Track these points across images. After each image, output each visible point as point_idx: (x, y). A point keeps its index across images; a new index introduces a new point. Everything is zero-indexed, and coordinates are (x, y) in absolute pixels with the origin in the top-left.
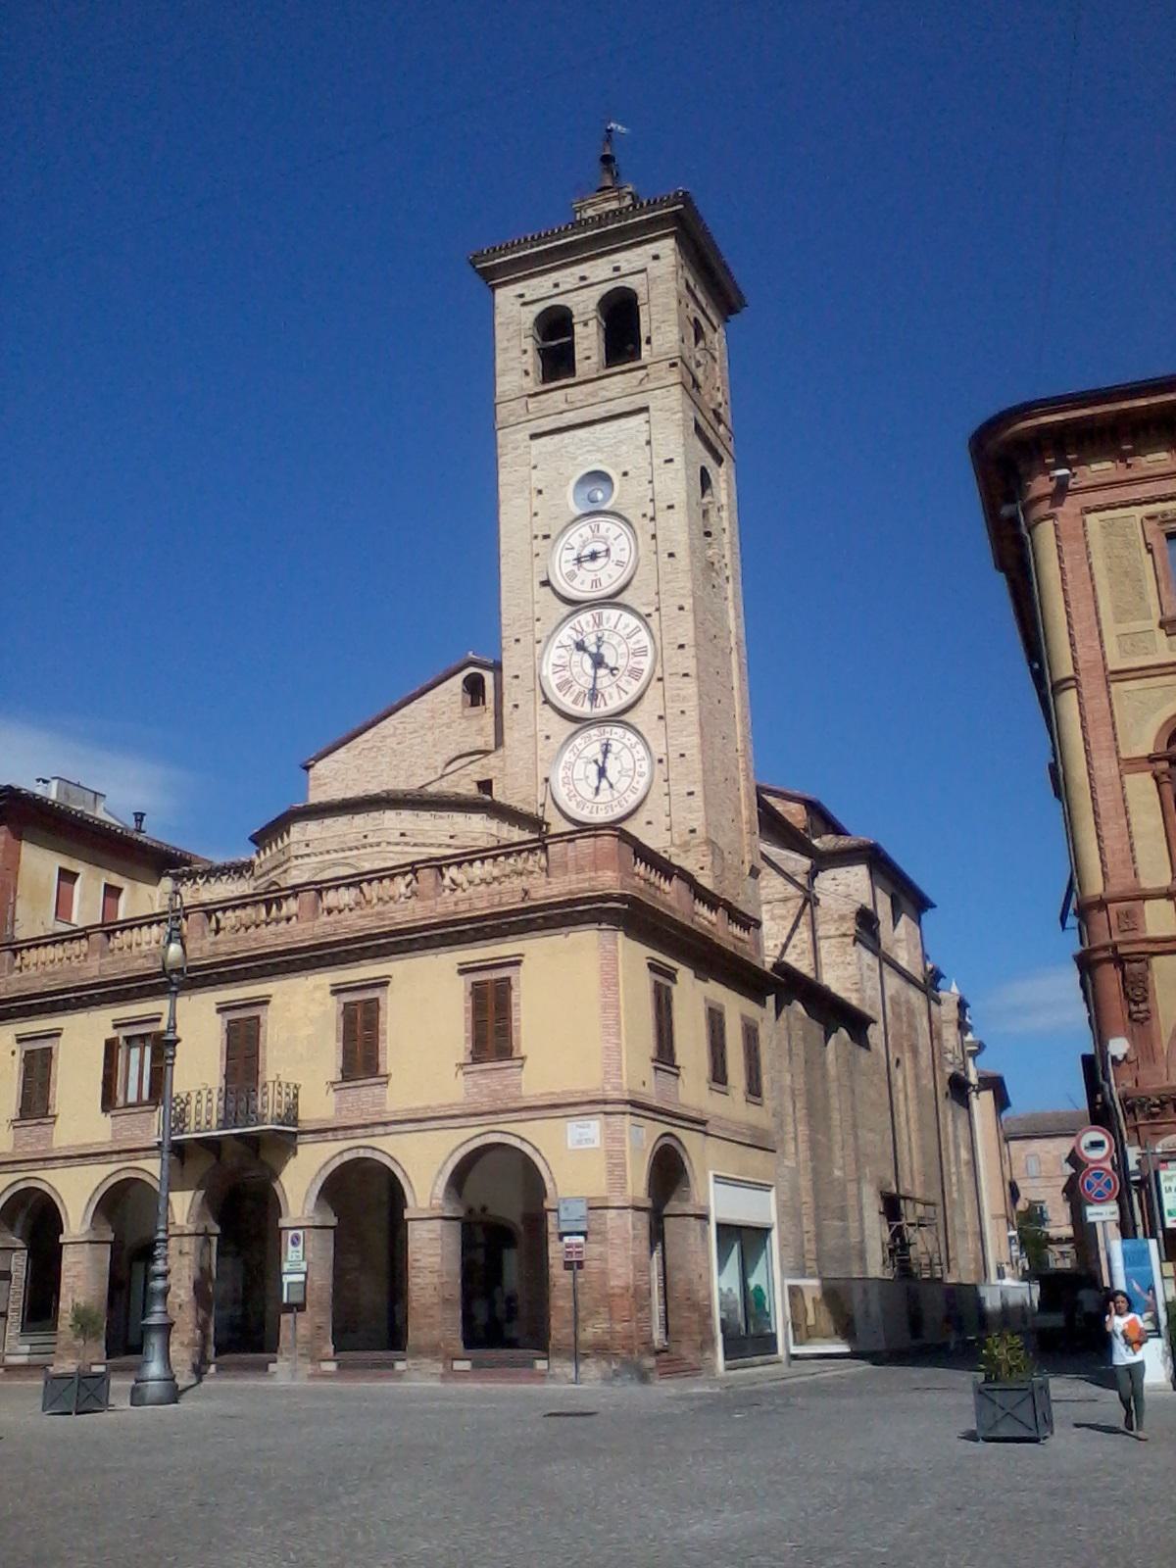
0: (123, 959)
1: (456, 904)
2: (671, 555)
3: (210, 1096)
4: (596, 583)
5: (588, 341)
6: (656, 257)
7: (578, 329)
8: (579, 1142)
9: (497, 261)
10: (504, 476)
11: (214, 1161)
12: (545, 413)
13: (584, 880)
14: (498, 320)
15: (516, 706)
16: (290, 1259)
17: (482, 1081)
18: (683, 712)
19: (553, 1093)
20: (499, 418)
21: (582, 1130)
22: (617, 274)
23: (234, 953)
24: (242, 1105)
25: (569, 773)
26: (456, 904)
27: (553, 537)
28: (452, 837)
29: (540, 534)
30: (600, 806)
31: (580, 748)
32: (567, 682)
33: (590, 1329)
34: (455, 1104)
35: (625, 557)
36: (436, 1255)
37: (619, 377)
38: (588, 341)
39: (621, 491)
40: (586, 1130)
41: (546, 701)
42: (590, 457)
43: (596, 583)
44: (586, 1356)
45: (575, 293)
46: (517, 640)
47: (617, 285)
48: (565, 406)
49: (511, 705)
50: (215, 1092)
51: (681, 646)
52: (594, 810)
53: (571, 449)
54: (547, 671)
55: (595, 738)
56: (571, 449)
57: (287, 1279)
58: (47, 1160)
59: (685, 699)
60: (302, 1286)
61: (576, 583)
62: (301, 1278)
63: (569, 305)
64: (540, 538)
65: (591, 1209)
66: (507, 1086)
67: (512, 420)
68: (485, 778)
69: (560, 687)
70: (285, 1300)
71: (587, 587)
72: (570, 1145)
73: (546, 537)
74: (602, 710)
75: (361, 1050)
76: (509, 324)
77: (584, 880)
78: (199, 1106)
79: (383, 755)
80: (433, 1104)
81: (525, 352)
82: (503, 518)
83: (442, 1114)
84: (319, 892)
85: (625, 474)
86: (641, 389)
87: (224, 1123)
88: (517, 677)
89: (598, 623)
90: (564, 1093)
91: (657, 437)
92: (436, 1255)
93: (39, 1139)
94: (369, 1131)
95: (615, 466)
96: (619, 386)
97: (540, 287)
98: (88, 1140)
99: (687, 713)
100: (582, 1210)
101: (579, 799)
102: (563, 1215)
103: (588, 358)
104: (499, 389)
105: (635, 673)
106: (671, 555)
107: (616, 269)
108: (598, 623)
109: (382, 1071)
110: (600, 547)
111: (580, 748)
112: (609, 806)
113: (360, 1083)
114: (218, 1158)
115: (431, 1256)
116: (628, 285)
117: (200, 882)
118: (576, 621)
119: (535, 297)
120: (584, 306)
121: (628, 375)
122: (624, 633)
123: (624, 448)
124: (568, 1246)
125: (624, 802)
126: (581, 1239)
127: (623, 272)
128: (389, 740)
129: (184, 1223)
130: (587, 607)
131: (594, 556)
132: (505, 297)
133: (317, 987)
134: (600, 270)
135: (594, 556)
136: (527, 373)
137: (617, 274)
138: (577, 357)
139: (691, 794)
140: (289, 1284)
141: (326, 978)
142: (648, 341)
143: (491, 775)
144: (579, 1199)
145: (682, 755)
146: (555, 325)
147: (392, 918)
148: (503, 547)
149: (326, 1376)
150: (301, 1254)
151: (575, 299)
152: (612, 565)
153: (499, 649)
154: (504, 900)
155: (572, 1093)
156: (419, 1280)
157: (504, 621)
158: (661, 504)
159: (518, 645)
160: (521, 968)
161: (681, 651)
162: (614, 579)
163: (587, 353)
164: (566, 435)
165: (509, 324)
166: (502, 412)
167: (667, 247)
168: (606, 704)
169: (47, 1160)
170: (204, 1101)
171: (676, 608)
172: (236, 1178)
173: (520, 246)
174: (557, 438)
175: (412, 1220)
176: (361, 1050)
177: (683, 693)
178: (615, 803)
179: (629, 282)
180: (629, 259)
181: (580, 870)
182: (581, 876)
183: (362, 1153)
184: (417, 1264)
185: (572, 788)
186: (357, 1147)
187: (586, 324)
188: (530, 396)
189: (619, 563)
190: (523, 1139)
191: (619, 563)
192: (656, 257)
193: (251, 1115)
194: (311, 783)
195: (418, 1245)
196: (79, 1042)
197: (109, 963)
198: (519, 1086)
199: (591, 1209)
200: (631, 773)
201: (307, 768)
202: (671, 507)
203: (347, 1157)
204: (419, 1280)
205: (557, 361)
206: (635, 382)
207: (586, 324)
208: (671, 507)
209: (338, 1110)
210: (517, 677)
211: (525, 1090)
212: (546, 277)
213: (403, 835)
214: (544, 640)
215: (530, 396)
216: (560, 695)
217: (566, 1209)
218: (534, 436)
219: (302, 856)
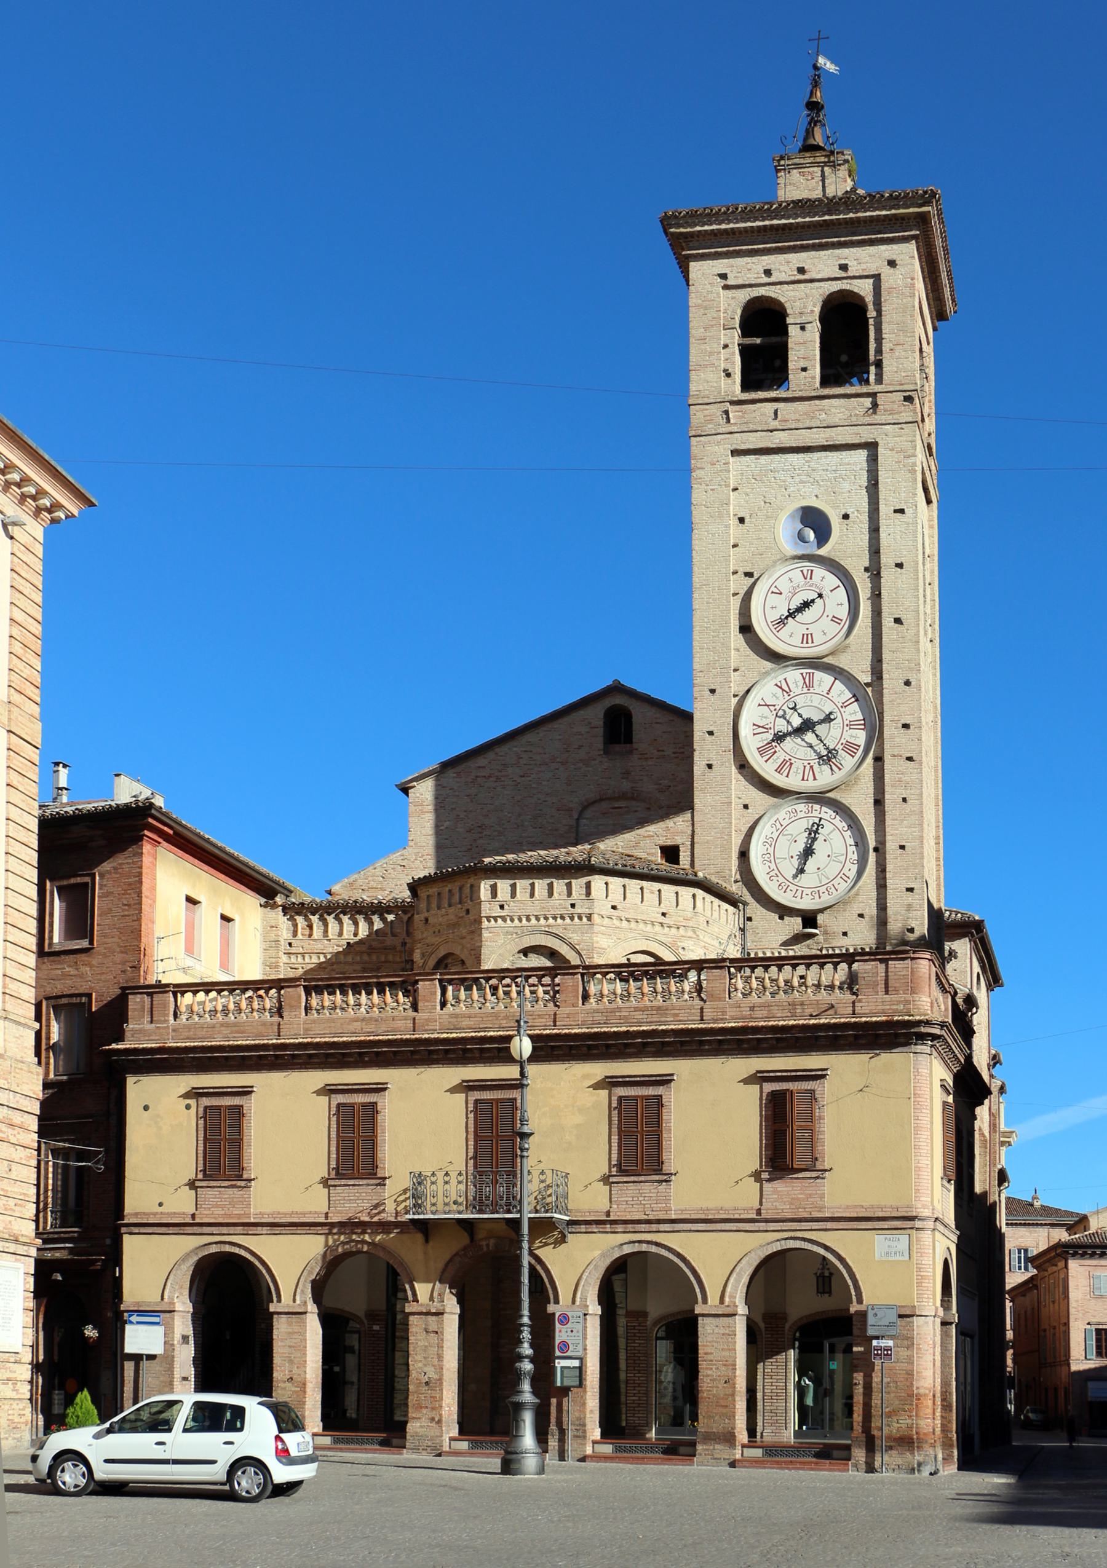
2: (898, 621)
3: (447, 1179)
4: (807, 638)
5: (805, 347)
6: (892, 263)
7: (793, 331)
9: (698, 228)
10: (698, 495)
11: (465, 1240)
12: (752, 427)
13: (899, 1002)
14: (693, 300)
15: (710, 766)
18: (904, 800)
19: (862, 1206)
20: (694, 421)
21: (888, 1243)
22: (843, 274)
23: (484, 1030)
24: (501, 1190)
25: (771, 851)
26: (752, 1009)
27: (756, 576)
28: (664, 914)
29: (741, 570)
30: (806, 891)
31: (784, 823)
37: (842, 401)
38: (805, 347)
39: (841, 537)
40: (895, 1244)
41: (743, 766)
42: (806, 490)
43: (807, 638)
44: (891, 1448)
45: (792, 287)
46: (713, 691)
47: (848, 287)
48: (775, 424)
50: (453, 1175)
51: (906, 726)
52: (799, 894)
53: (780, 475)
55: (802, 815)
56: (780, 475)
57: (559, 1364)
58: (250, 1226)
61: (784, 633)
62: (576, 1363)
63: (783, 300)
64: (740, 574)
65: (900, 1316)
67: (710, 428)
68: (669, 843)
69: (761, 751)
70: (559, 1384)
71: (797, 640)
72: (877, 1257)
73: (749, 575)
74: (810, 785)
75: (639, 1145)
76: (706, 308)
77: (899, 1002)
78: (447, 1186)
79: (504, 787)
80: (727, 1206)
82: (696, 544)
83: (737, 1216)
85: (846, 517)
86: (867, 420)
87: (479, 1204)
88: (711, 733)
89: (809, 685)
90: (872, 1207)
93: (233, 1204)
94: (654, 1227)
95: (835, 507)
96: (841, 411)
97: (747, 269)
98: (298, 1209)
99: (909, 802)
104: (693, 388)
105: (850, 748)
106: (898, 621)
107: (844, 267)
108: (809, 685)
109: (666, 1168)
110: (813, 595)
111: (784, 823)
112: (816, 892)
113: (642, 1178)
114: (472, 1240)
116: (856, 290)
118: (781, 678)
119: (740, 282)
120: (804, 307)
121: (854, 401)
123: (846, 486)
125: (833, 890)
127: (850, 274)
128: (510, 770)
130: (797, 665)
132: (703, 272)
134: (823, 263)
136: (728, 375)
137: (843, 274)
138: (791, 365)
139: (910, 890)
141: (599, 1069)
142: (879, 364)
143: (678, 840)
144: (890, 1307)
145: (902, 847)
146: (764, 322)
148: (696, 580)
149: (606, 1458)
151: (791, 294)
152: (826, 622)
153: (692, 699)
156: (709, 1372)
157: (696, 666)
159: (712, 698)
160: (826, 1082)
161: (903, 730)
163: (802, 364)
164: (776, 457)
165: (706, 308)
166: (697, 416)
167: (908, 254)
168: (815, 779)
169: (250, 1226)
170: (440, 1182)
171: (902, 682)
172: (492, 1265)
173: (726, 217)
174: (764, 459)
175: (703, 1315)
176: (639, 1145)
177: (906, 778)
178: (823, 889)
179: (864, 288)
180: (864, 259)
183: (644, 1247)
184: (709, 1357)
185: (773, 866)
186: (640, 1242)
187: (803, 328)
188: (732, 403)
190: (826, 1248)
192: (892, 263)
193: (513, 1202)
194: (412, 808)
195: (710, 1339)
198: (822, 1196)
199: (900, 1316)
200: (843, 859)
201: (405, 790)
202: (900, 566)
203: (628, 1250)
204: (709, 1372)
205: (764, 366)
206: (862, 411)
207: (803, 328)
208: (900, 566)
210: (711, 733)
211: (828, 1202)
212: (755, 259)
213: (614, 907)
215: (732, 403)
216: (762, 760)
218: (735, 453)
219: (495, 919)
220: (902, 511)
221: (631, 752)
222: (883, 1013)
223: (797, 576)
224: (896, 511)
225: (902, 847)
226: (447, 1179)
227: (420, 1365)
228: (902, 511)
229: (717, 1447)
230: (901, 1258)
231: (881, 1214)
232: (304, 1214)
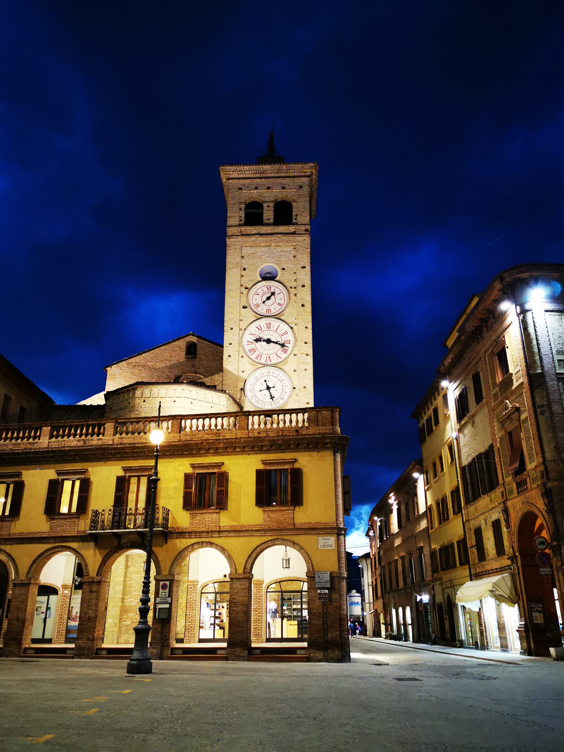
0: (64, 441)
1: (259, 433)
4: (268, 310)
8: (324, 546)
13: (327, 429)
15: (230, 356)
16: (160, 596)
17: (272, 515)
25: (253, 388)
30: (266, 403)
32: (253, 349)
33: (330, 635)
34: (257, 525)
35: (282, 302)
36: (245, 596)
40: (327, 541)
43: (268, 310)
46: (232, 329)
49: (227, 355)
54: (245, 343)
59: (307, 364)
60: (167, 611)
66: (286, 518)
69: (250, 351)
81: (240, 209)
84: (181, 420)
85: (283, 269)
90: (316, 523)
91: (299, 256)
92: (245, 596)
100: (327, 577)
101: (256, 399)
102: (317, 579)
103: (269, 220)
115: (242, 597)
117: (63, 412)
122: (281, 333)
123: (283, 259)
124: (320, 594)
126: (327, 591)
129: (95, 576)
131: (268, 298)
133: (180, 465)
135: (268, 298)
140: (159, 608)
145: (305, 387)
147: (225, 436)
150: (167, 594)
152: (276, 305)
154: (284, 434)
155: (320, 523)
158: (300, 283)
162: (277, 310)
181: (324, 425)
182: (324, 428)
185: (253, 394)
189: (279, 304)
191: (279, 304)
196: (37, 480)
197: (55, 442)
200: (281, 391)
202: (303, 286)
209: (192, 524)
214: (243, 330)
217: (319, 577)
220: (304, 267)
221: (196, 358)
222: (319, 434)
223: (265, 289)
224: (303, 267)
225: (305, 387)
226: (110, 512)
227: (86, 609)
228: (304, 267)
229: (238, 649)
230: (330, 548)
231: (320, 527)
232: (36, 533)
